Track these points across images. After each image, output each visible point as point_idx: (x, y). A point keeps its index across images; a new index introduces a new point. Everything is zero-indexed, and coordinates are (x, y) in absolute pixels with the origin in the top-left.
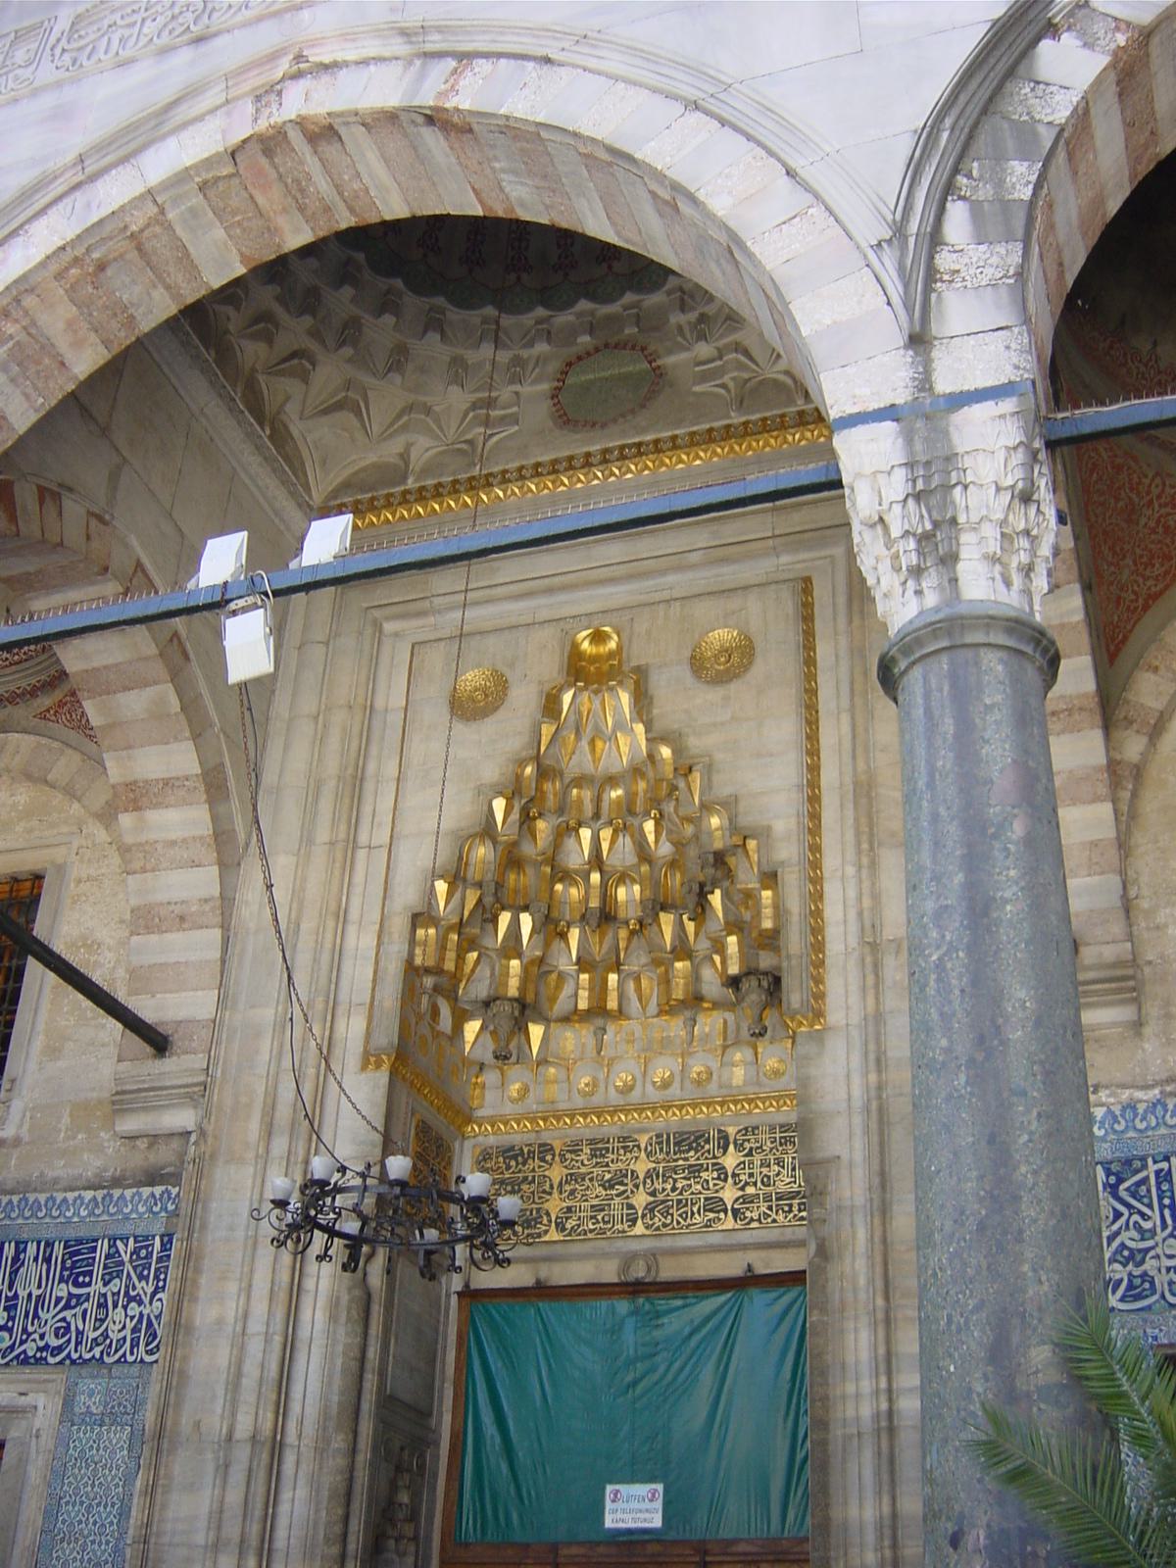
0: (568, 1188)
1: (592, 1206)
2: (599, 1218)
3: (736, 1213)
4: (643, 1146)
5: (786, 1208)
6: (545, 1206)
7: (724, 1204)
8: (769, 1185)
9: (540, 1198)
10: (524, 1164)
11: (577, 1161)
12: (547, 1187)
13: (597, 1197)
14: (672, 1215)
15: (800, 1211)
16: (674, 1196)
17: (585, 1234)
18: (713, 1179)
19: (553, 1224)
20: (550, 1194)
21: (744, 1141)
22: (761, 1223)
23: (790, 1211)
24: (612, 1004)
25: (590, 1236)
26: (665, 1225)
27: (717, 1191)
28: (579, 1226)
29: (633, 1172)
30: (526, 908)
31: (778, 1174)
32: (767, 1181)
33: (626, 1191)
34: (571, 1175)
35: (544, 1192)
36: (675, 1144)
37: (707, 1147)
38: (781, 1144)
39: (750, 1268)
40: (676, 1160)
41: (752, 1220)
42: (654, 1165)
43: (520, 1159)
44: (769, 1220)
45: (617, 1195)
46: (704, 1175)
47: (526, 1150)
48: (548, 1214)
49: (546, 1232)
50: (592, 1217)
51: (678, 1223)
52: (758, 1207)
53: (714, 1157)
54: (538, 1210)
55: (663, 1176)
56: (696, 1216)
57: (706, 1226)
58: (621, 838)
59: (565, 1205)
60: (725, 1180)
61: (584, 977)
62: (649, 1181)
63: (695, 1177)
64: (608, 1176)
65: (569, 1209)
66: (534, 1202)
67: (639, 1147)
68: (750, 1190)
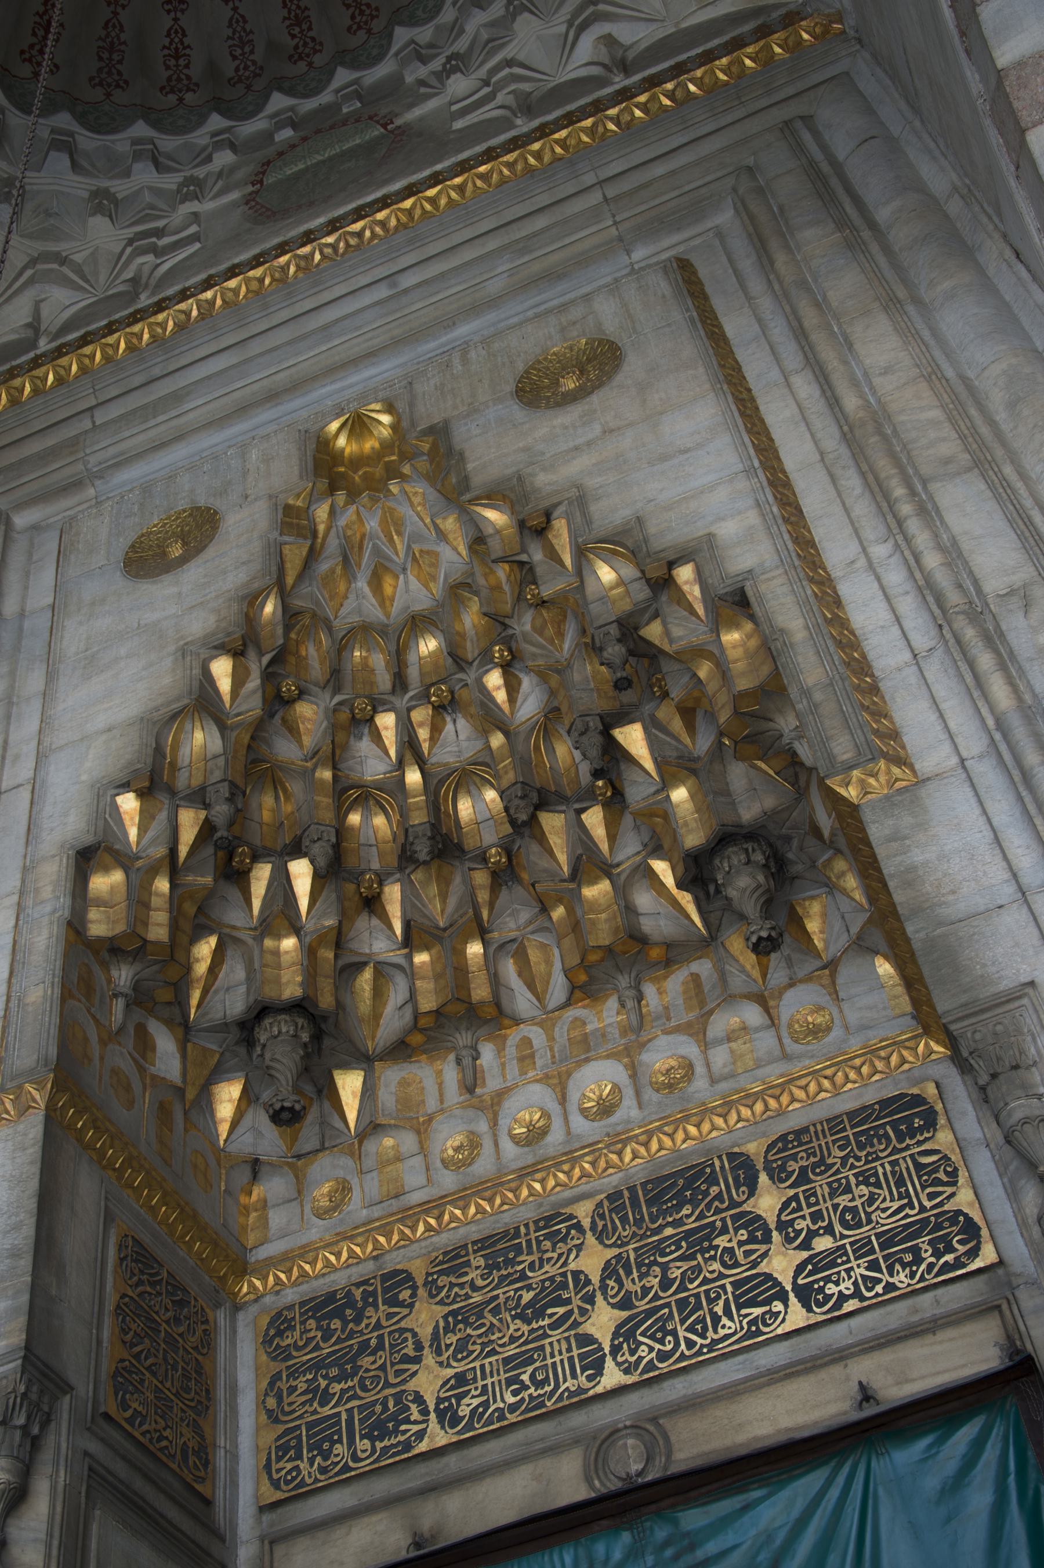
0: (451, 1339)
1: (506, 1361)
2: (525, 1377)
3: (806, 1296)
4: (586, 1223)
5: (908, 1258)
6: (412, 1385)
7: (777, 1283)
8: (859, 1225)
9: (398, 1373)
10: (358, 1320)
11: (461, 1286)
12: (410, 1350)
13: (513, 1339)
14: (674, 1333)
15: (937, 1254)
16: (669, 1296)
17: (502, 1417)
18: (741, 1244)
19: (433, 1416)
20: (417, 1360)
21: (785, 1160)
22: (863, 1299)
23: (918, 1260)
24: (480, 992)
25: (512, 1418)
26: (663, 1356)
27: (755, 1264)
28: (486, 1405)
29: (576, 1274)
30: (296, 850)
31: (871, 1199)
32: (852, 1219)
33: (570, 1312)
34: (454, 1313)
35: (407, 1359)
36: (650, 1203)
37: (714, 1190)
38: (861, 1147)
39: (866, 1395)
40: (661, 1228)
41: (842, 1298)
42: (616, 1251)
43: (348, 1312)
44: (879, 1289)
45: (553, 1326)
46: (722, 1242)
47: (358, 1293)
48: (419, 1399)
49: (420, 1435)
50: (509, 1382)
51: (690, 1344)
52: (848, 1271)
53: (734, 1204)
54: (398, 1397)
55: (639, 1266)
56: (725, 1320)
57: (749, 1335)
58: (449, 727)
59: (449, 1372)
60: (767, 1239)
61: (421, 958)
62: (611, 1283)
63: (703, 1251)
64: (527, 1296)
65: (461, 1379)
66: (387, 1385)
67: (578, 1227)
68: (823, 1243)
